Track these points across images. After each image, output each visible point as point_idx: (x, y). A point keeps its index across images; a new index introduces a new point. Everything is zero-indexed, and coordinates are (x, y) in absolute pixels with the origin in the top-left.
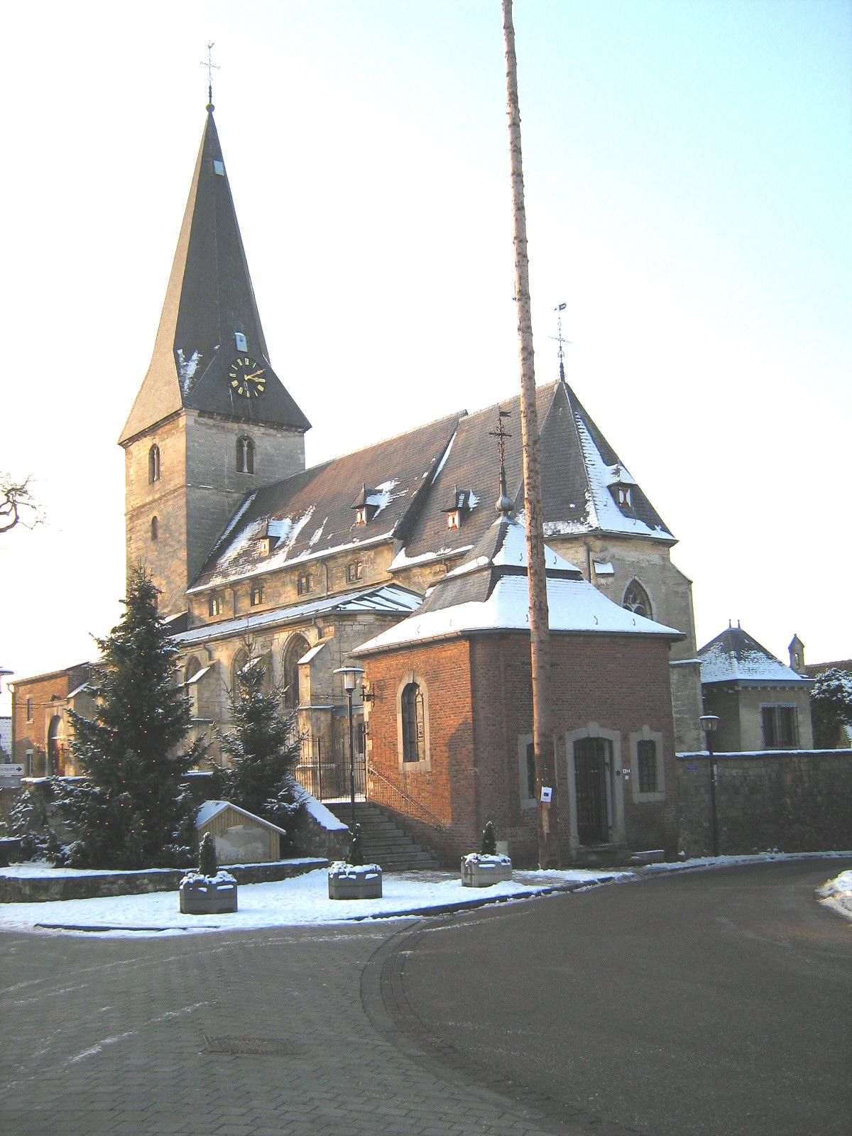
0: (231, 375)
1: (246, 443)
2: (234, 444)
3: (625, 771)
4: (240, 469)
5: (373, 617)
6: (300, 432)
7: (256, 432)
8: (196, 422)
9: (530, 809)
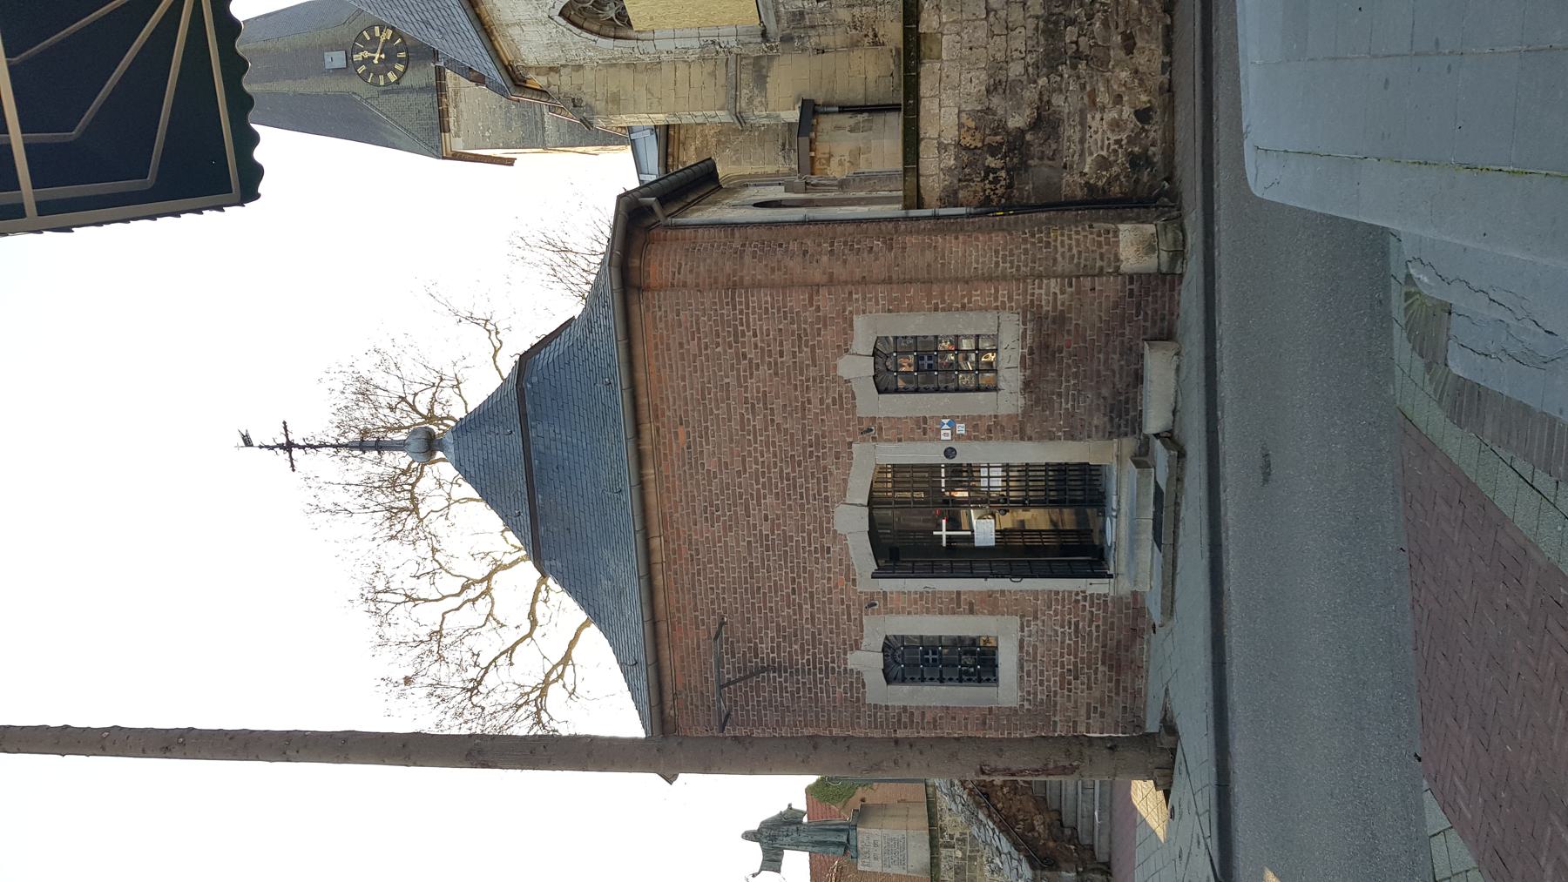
0: (382, 83)
3: (946, 434)
8: (457, 135)
9: (1022, 689)
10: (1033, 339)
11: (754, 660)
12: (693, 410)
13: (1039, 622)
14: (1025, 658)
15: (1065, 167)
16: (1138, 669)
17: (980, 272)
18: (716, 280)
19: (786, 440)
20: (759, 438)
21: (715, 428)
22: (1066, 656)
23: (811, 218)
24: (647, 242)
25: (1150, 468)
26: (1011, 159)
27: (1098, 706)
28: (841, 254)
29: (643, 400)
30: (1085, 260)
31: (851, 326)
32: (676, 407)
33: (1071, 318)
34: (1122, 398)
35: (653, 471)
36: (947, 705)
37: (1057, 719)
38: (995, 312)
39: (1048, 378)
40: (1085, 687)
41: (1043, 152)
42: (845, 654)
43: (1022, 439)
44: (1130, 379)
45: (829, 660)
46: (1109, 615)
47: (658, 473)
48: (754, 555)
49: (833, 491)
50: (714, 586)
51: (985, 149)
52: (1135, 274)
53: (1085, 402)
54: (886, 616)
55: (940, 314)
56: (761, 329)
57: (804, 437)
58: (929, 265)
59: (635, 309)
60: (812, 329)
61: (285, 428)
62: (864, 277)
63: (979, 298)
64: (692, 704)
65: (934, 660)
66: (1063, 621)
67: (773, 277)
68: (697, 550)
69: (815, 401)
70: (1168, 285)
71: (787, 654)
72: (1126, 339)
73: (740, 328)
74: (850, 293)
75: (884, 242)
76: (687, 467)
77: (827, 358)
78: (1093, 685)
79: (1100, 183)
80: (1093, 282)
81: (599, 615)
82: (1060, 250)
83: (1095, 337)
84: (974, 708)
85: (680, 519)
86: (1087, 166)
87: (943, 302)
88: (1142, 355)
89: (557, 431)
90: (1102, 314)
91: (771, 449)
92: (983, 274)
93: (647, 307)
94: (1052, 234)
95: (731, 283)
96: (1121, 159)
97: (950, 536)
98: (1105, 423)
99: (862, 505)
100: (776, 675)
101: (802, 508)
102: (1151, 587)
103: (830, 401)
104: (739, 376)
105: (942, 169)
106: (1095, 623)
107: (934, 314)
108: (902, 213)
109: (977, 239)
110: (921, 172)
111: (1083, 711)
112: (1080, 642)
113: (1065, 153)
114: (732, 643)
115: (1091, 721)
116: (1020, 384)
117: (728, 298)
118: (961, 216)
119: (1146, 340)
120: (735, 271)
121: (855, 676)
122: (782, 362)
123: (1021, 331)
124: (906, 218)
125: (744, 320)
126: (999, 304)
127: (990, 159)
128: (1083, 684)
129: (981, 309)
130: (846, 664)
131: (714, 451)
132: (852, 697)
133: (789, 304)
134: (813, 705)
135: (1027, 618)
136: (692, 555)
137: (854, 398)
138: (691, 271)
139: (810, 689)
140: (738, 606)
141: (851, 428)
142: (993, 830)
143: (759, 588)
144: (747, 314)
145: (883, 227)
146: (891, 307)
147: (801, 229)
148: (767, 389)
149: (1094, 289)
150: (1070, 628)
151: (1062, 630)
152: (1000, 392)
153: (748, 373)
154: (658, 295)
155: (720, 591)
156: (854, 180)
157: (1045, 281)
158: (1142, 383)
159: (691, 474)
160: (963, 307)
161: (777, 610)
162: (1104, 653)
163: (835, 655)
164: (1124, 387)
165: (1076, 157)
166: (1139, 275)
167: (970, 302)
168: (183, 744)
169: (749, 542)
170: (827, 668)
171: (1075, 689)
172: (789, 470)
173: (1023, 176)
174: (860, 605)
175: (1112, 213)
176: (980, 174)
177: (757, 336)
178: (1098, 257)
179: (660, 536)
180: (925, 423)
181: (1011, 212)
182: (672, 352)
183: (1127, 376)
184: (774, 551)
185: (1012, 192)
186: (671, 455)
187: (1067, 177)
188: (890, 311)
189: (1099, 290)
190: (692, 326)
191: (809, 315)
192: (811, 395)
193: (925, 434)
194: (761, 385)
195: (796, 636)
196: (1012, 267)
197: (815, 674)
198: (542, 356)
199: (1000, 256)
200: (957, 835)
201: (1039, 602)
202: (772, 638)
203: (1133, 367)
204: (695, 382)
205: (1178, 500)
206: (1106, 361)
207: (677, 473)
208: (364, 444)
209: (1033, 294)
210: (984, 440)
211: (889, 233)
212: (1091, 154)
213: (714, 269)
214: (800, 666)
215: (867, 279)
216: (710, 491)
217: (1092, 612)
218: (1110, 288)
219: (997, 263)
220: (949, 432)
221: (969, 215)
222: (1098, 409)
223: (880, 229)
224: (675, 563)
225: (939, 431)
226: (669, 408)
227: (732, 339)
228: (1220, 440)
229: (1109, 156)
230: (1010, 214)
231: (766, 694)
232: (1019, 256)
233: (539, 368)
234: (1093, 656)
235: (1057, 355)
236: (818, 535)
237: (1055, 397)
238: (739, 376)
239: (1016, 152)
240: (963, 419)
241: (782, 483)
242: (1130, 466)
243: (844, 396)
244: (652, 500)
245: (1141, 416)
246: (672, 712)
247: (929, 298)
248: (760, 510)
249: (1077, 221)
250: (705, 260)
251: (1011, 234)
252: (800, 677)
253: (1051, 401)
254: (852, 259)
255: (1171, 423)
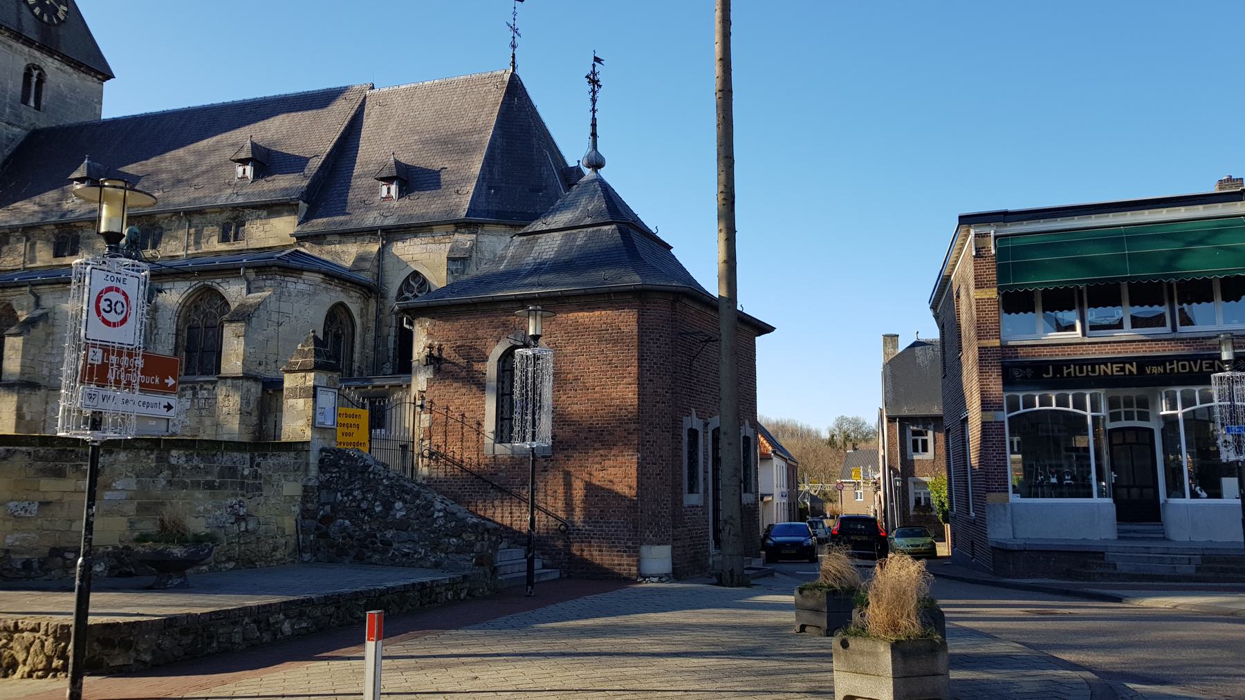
1: (35, 73)
2: (22, 71)
4: (25, 100)
5: (322, 276)
6: (99, 79)
7: (51, 65)
200: (260, 471)
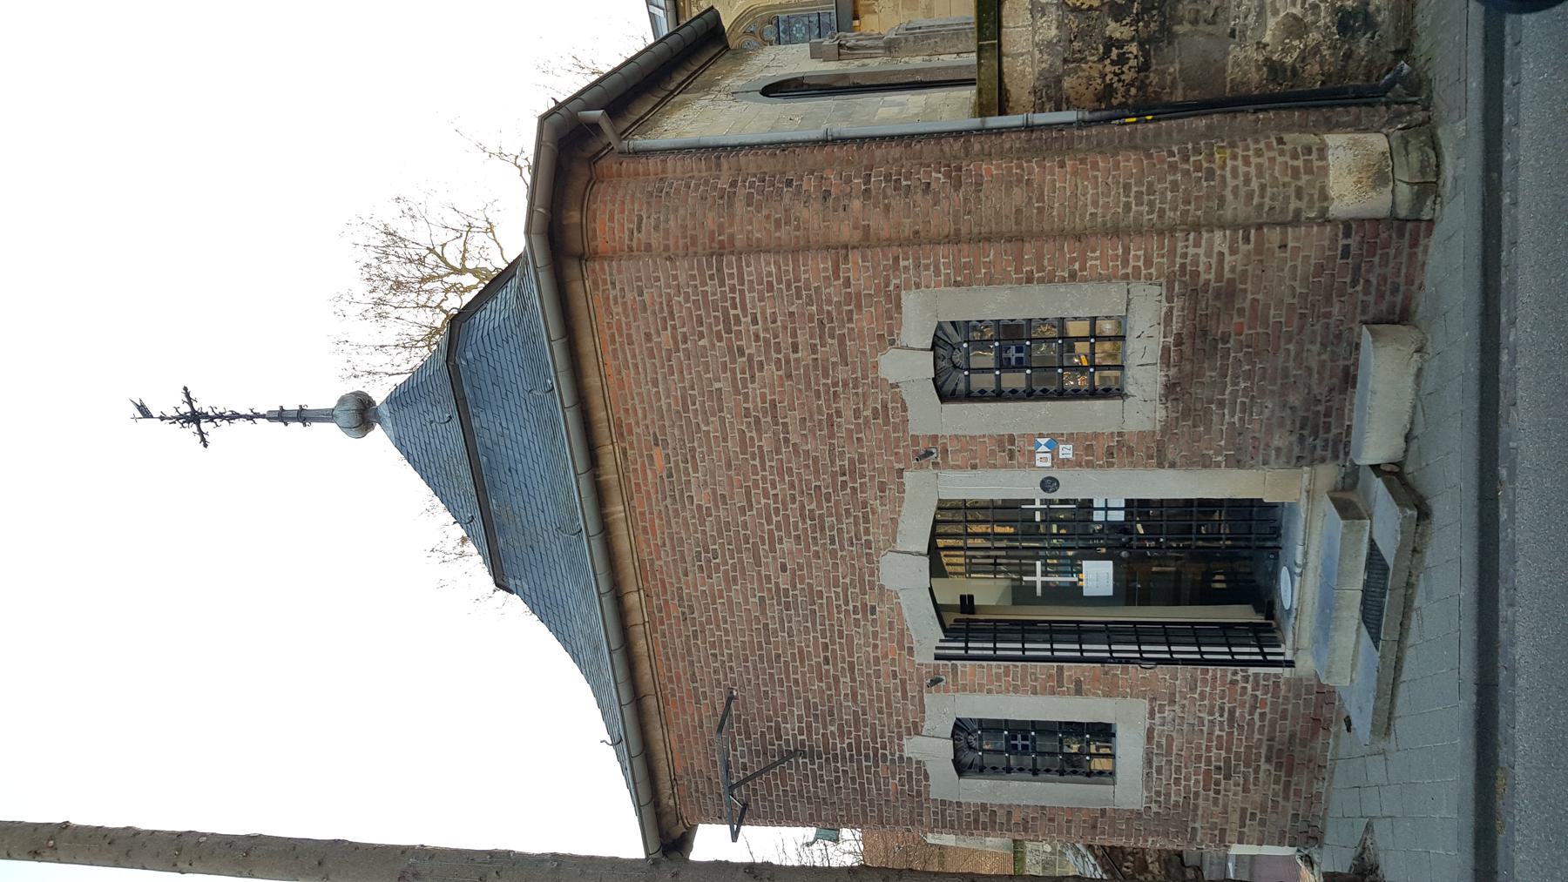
3: (1043, 460)
9: (1148, 788)
10: (1183, 322)
11: (776, 742)
12: (672, 426)
13: (1176, 707)
14: (1155, 751)
15: (1233, 34)
16: (1318, 769)
17: (1100, 220)
18: (694, 239)
19: (807, 466)
20: (768, 464)
21: (705, 449)
22: (1215, 751)
23: (836, 135)
24: (592, 182)
25: (1364, 518)
26: (1147, 25)
27: (1258, 812)
28: (881, 197)
29: (600, 415)
30: (1272, 199)
31: (899, 307)
32: (648, 421)
33: (1245, 291)
34: (1321, 408)
35: (622, 508)
36: (1043, 804)
37: (1197, 825)
38: (1123, 283)
39: (1203, 380)
40: (1240, 788)
41: (1198, 11)
42: (900, 738)
43: (1160, 465)
44: (1335, 380)
45: (879, 746)
46: (1280, 700)
47: (629, 509)
48: (769, 614)
49: (877, 534)
50: (717, 652)
51: (1106, 8)
52: (1355, 220)
53: (1261, 413)
54: (957, 695)
55: (1035, 288)
56: (763, 313)
57: (833, 462)
58: (1018, 211)
59: (576, 288)
60: (840, 313)
61: (187, 395)
62: (917, 232)
63: (1098, 262)
64: (697, 791)
65: (1025, 747)
66: (1213, 707)
67: (777, 234)
68: (691, 607)
69: (848, 414)
70: (1407, 236)
71: (820, 736)
72: (1332, 321)
73: (732, 312)
74: (896, 259)
75: (948, 175)
76: (669, 501)
77: (864, 353)
78: (1252, 787)
79: (1288, 60)
80: (1284, 234)
81: (578, 656)
82: (1230, 182)
83: (1283, 320)
84: (1079, 809)
85: (665, 568)
86: (1269, 32)
87: (1041, 269)
88: (1358, 346)
89: (504, 425)
90: (1297, 284)
91: (787, 478)
92: (1104, 224)
93: (595, 283)
94: (1217, 156)
95: (715, 245)
96: (1325, 19)
97: (1047, 582)
98: (1291, 443)
99: (921, 554)
100: (807, 760)
101: (833, 553)
102: (1352, 681)
103: (868, 413)
104: (734, 379)
105: (1037, 44)
106: (1258, 710)
107: (1025, 287)
108: (976, 122)
109: (1095, 166)
110: (1004, 49)
111: (1235, 818)
112: (1236, 734)
113: (1233, 13)
114: (746, 721)
115: (1245, 830)
116: (1159, 389)
117: (711, 269)
118: (1069, 124)
119: (1366, 323)
120: (721, 226)
121: (914, 766)
122: (795, 360)
123: (1164, 310)
124: (983, 132)
125: (738, 300)
126: (1130, 270)
127: (1112, 25)
128: (1237, 784)
129: (1100, 279)
130: (901, 750)
131: (705, 481)
132: (911, 789)
133: (803, 276)
134: (859, 797)
135: (1158, 702)
136: (683, 613)
137: (905, 409)
138: (656, 228)
139: (853, 779)
140: (751, 676)
141: (901, 451)
142: (1094, 865)
143: (778, 656)
144: (742, 292)
145: (946, 148)
146: (959, 279)
147: (820, 155)
148: (776, 397)
149: (1285, 246)
150: (1221, 716)
151: (1211, 718)
152: (1128, 400)
153: (747, 376)
154: (610, 267)
155: (725, 658)
156: (906, 40)
157: (1205, 235)
158: (1354, 386)
159: (676, 511)
160: (1073, 276)
161: (805, 684)
162: (1270, 748)
163: (886, 739)
164: (1325, 394)
165: (1251, 19)
166: (1361, 221)
167: (1083, 268)
168: (54, 848)
169: (762, 599)
170: (876, 755)
171: (1225, 790)
172: (814, 506)
173: (1166, 50)
174: (921, 679)
175: (1313, 116)
176: (1097, 49)
177: (757, 324)
178: (1293, 195)
179: (639, 591)
180: (1012, 443)
181: (1149, 118)
182: (636, 346)
183: (1331, 377)
184: (796, 609)
185: (1147, 77)
186: (646, 486)
187: (1235, 52)
188: (957, 284)
189: (1293, 248)
190: (662, 309)
191: (834, 291)
192: (841, 404)
193: (1011, 459)
194: (767, 391)
195: (831, 714)
196: (1151, 212)
197: (859, 761)
198: (477, 320)
199: (1132, 194)
201: (1178, 682)
202: (800, 718)
203: (1341, 363)
204: (673, 388)
205: (1413, 579)
206: (1298, 355)
207: (655, 509)
208: (284, 415)
209: (1185, 255)
210: (1101, 466)
211: (956, 158)
212: (1275, 12)
213: (689, 223)
214: (838, 751)
215: (922, 234)
216: (704, 532)
217: (1257, 696)
218: (1310, 244)
219: (1127, 206)
220: (1049, 456)
221: (1083, 124)
222: (1281, 424)
223: (942, 150)
224: (662, 623)
225: (1032, 454)
226: (637, 423)
227: (721, 327)
228: (1503, 516)
229: (1304, 16)
230: (1147, 121)
231: (795, 783)
232: (1163, 194)
233: (473, 342)
234: (1254, 751)
235: (1220, 346)
236: (857, 590)
237: (1214, 407)
238: (734, 379)
239: (1154, 12)
240: (1070, 438)
241: (804, 522)
242: (1327, 506)
243: (890, 406)
244: (623, 544)
245: (1348, 434)
246: (671, 802)
247: (1019, 261)
248: (774, 558)
249: (1256, 132)
250: (677, 210)
251: (1149, 156)
252: (839, 765)
253: (1208, 411)
254: (897, 203)
255: (1400, 454)
